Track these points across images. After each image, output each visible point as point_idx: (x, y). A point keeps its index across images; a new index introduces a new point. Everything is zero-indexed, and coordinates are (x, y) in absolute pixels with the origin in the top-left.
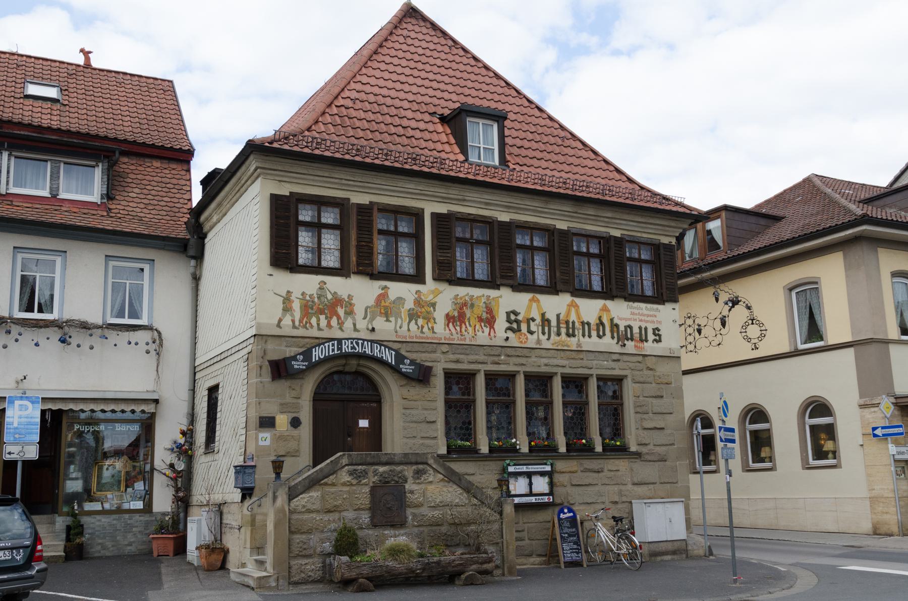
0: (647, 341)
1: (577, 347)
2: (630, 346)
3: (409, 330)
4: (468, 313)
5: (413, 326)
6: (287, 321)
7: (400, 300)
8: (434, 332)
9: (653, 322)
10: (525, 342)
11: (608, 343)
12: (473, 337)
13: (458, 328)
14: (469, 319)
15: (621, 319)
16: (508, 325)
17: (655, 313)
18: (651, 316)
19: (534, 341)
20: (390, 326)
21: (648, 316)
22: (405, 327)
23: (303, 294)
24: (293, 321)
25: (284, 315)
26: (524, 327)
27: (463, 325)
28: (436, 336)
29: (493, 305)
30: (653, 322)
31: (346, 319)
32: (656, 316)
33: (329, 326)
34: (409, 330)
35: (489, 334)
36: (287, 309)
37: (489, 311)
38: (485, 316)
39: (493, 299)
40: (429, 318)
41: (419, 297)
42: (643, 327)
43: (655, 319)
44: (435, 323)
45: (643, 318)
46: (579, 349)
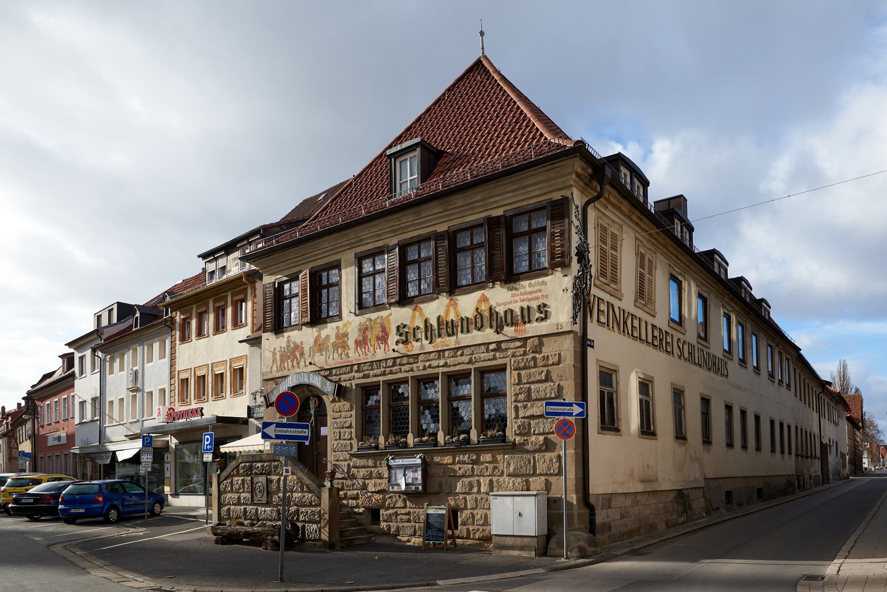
0: (530, 321)
1: (455, 345)
2: (509, 331)
3: (333, 359)
4: (369, 334)
5: (336, 356)
6: (275, 369)
7: (328, 336)
8: (349, 357)
9: (537, 298)
10: (411, 350)
11: (489, 335)
12: (373, 354)
13: (363, 349)
14: (370, 340)
15: (499, 305)
16: (398, 337)
17: (543, 287)
18: (535, 292)
19: (418, 348)
20: (323, 358)
21: (531, 293)
22: (331, 357)
23: (281, 348)
24: (277, 367)
25: (273, 365)
26: (411, 338)
27: (367, 347)
28: (350, 359)
29: (386, 322)
30: (537, 298)
31: (300, 359)
32: (540, 291)
33: (293, 366)
34: (333, 359)
35: (385, 350)
36: (274, 361)
37: (384, 329)
38: (380, 334)
39: (386, 317)
40: (345, 346)
41: (338, 332)
42: (525, 306)
43: (539, 294)
44: (349, 349)
45: (525, 297)
46: (457, 346)
